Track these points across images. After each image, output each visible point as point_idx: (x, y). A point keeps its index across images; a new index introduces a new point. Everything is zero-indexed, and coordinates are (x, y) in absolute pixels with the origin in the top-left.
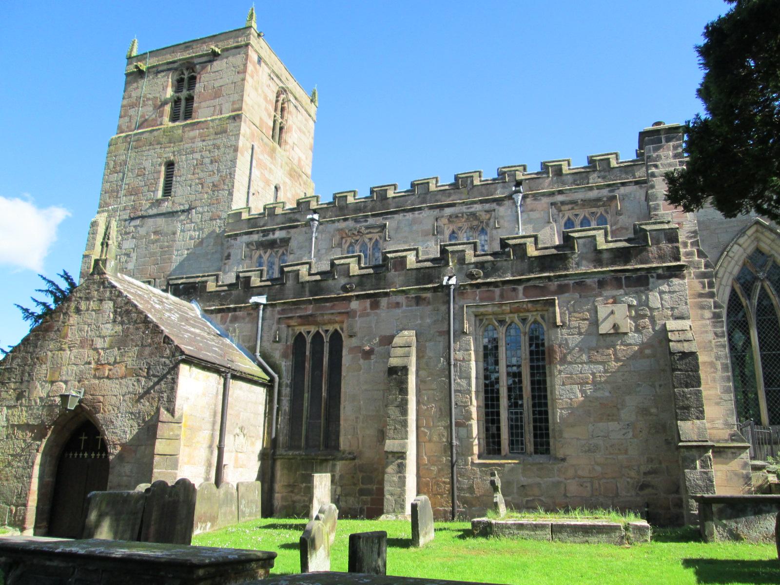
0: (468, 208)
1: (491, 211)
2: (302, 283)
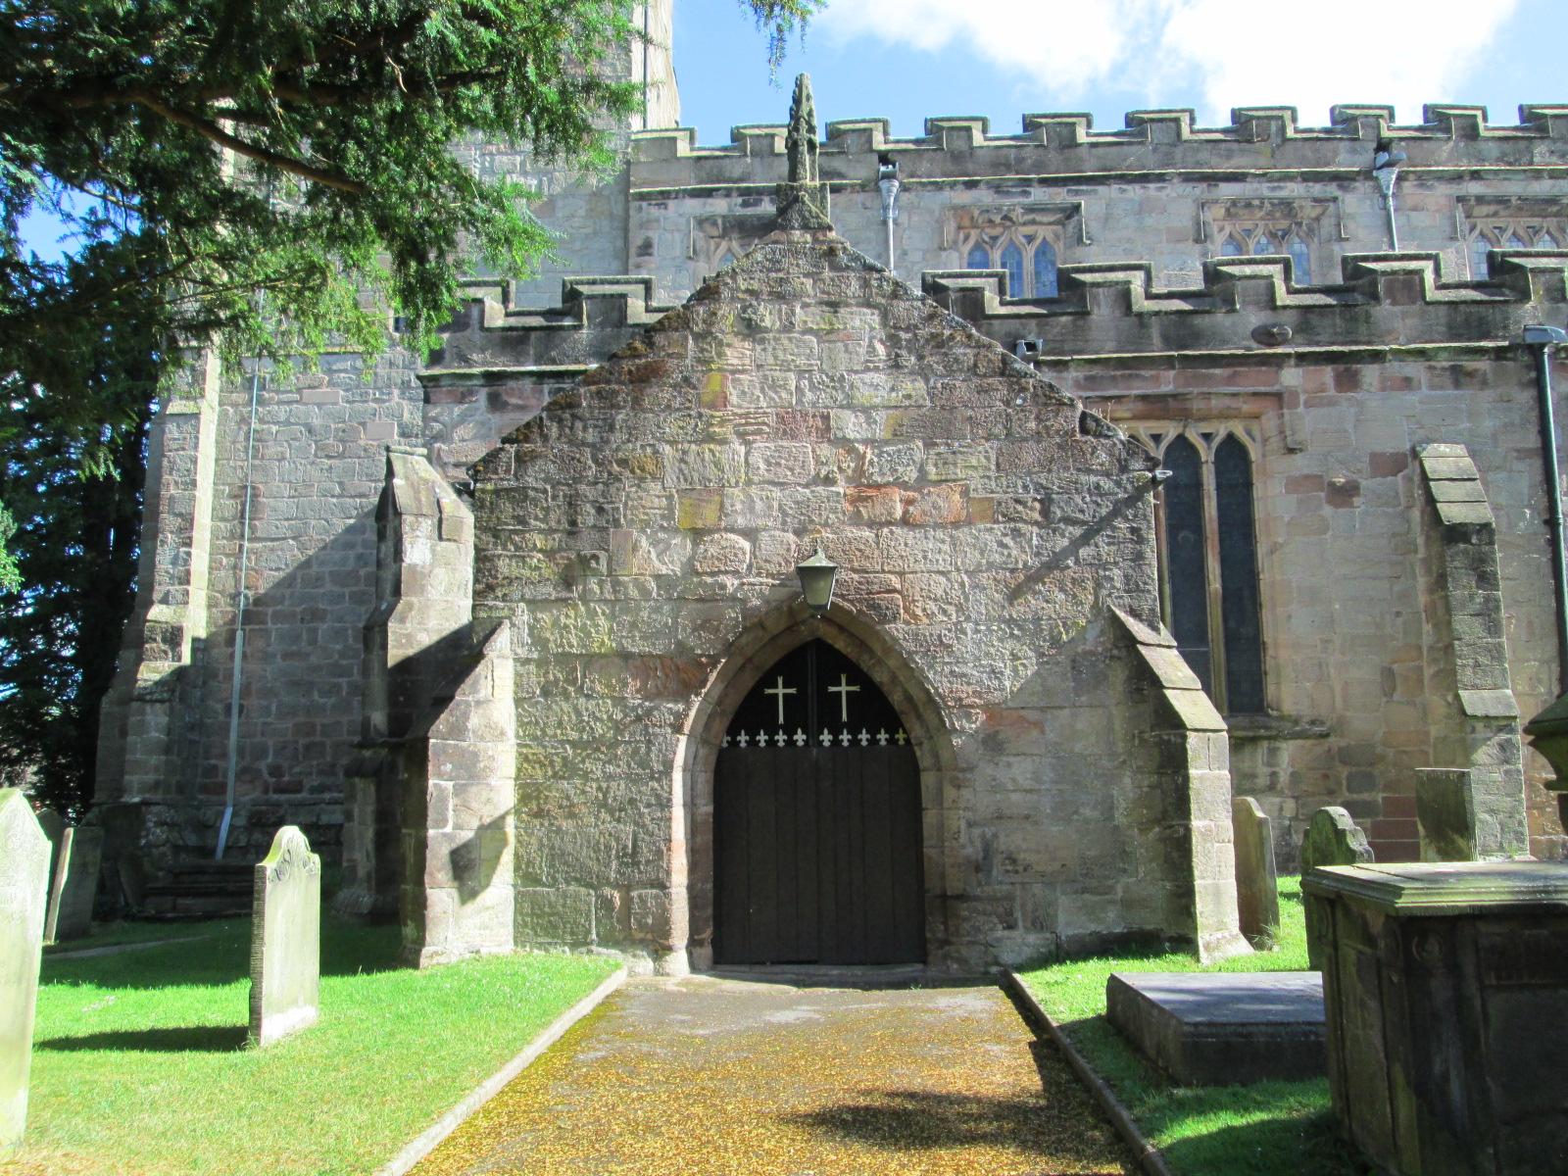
0: (1274, 189)
1: (1327, 200)
2: (1140, 315)
